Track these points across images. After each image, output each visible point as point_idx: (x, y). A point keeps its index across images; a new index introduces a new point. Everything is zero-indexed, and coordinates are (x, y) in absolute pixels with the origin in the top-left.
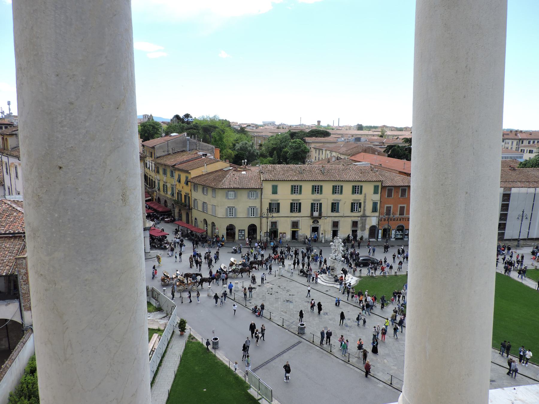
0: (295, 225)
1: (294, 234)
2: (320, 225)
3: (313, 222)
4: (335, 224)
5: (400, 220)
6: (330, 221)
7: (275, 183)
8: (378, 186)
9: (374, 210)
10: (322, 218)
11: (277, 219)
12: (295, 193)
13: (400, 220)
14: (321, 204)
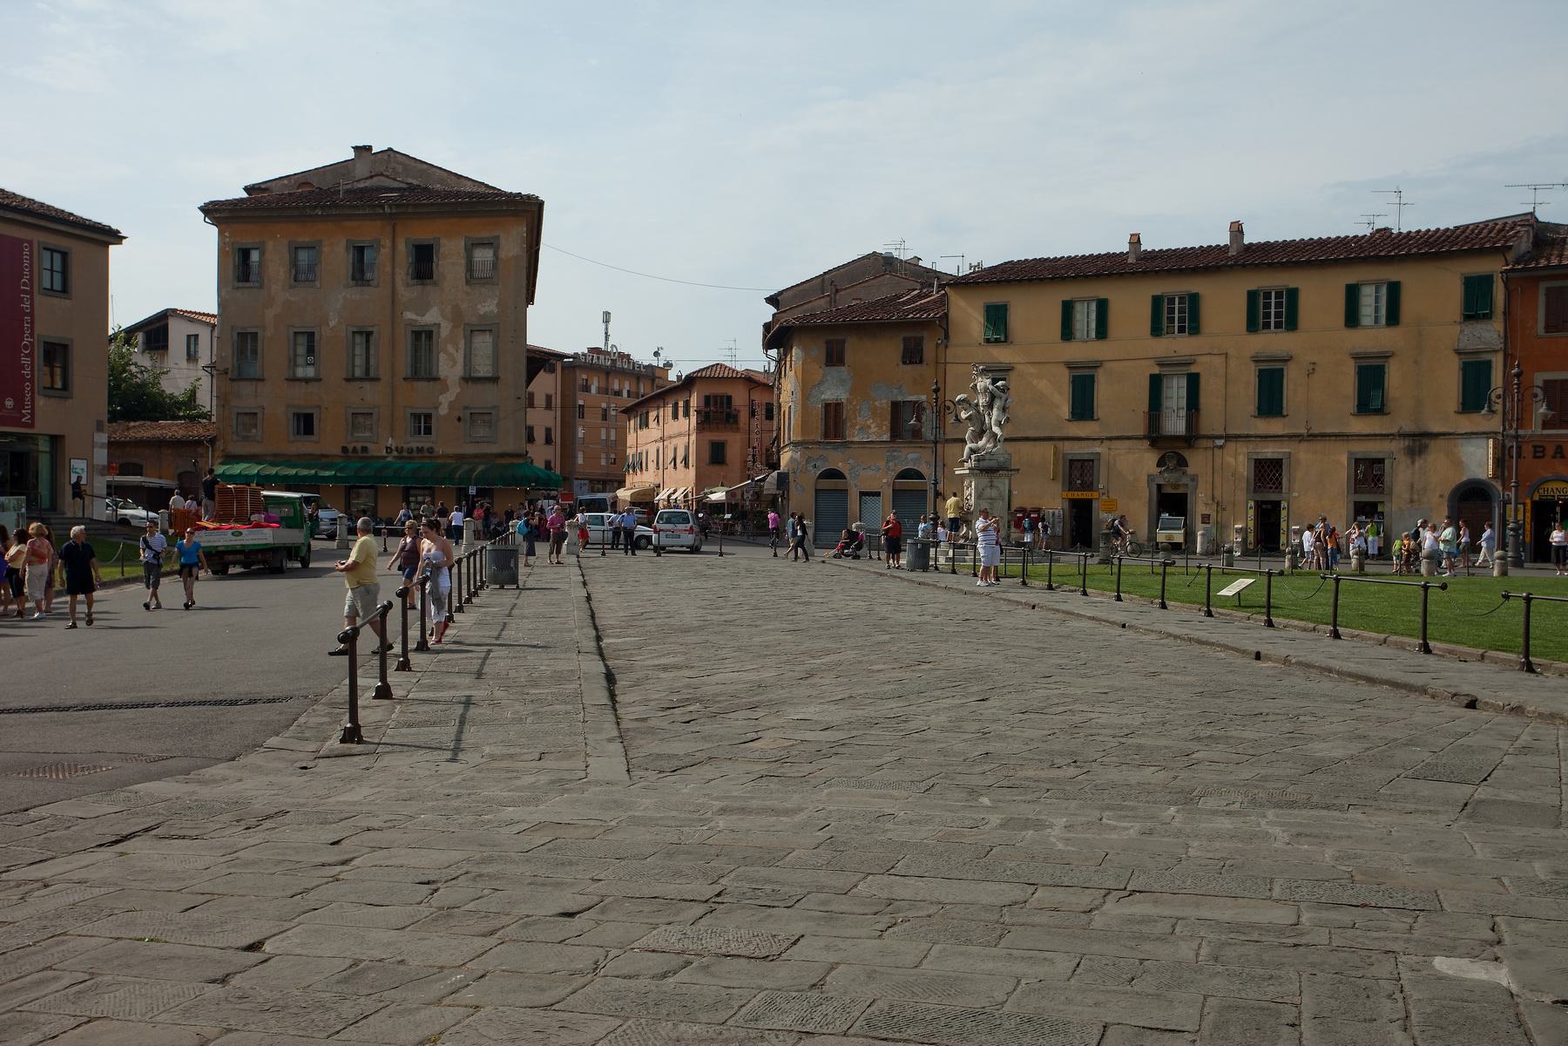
0: (1080, 472)
1: (1081, 513)
2: (1194, 478)
4: (1268, 473)
8: (1487, 280)
9: (1474, 395)
12: (1267, 326)
14: (1194, 382)
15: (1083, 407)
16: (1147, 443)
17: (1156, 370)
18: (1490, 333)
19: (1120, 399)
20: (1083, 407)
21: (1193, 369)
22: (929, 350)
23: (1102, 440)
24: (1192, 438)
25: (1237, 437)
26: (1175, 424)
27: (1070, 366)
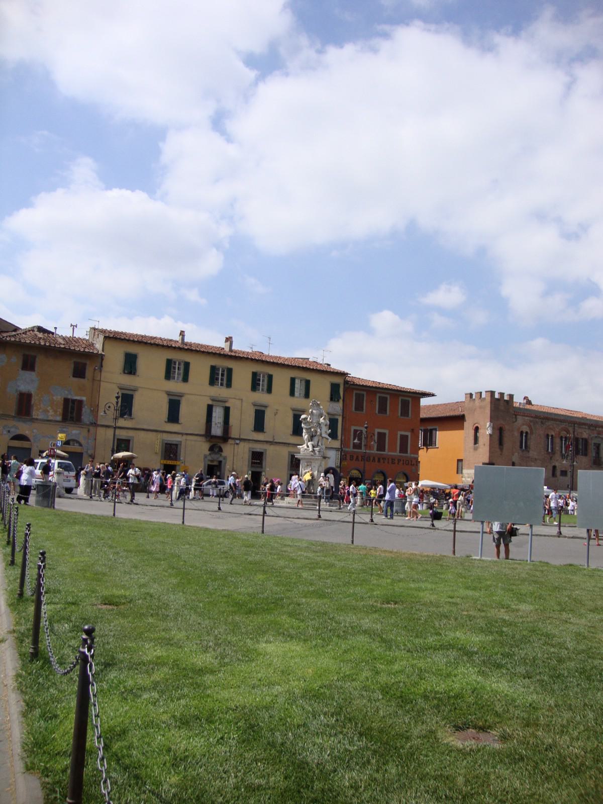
2: (225, 458)
3: (211, 449)
4: (257, 458)
5: (379, 461)
6: (247, 450)
7: (132, 349)
10: (230, 441)
11: (131, 434)
13: (379, 461)
14: (227, 411)
15: (173, 415)
16: (203, 439)
17: (210, 403)
18: (338, 407)
19: (192, 415)
20: (173, 415)
21: (227, 405)
22: (89, 372)
23: (182, 434)
24: (226, 437)
25: (244, 440)
26: (217, 430)
27: (169, 394)
